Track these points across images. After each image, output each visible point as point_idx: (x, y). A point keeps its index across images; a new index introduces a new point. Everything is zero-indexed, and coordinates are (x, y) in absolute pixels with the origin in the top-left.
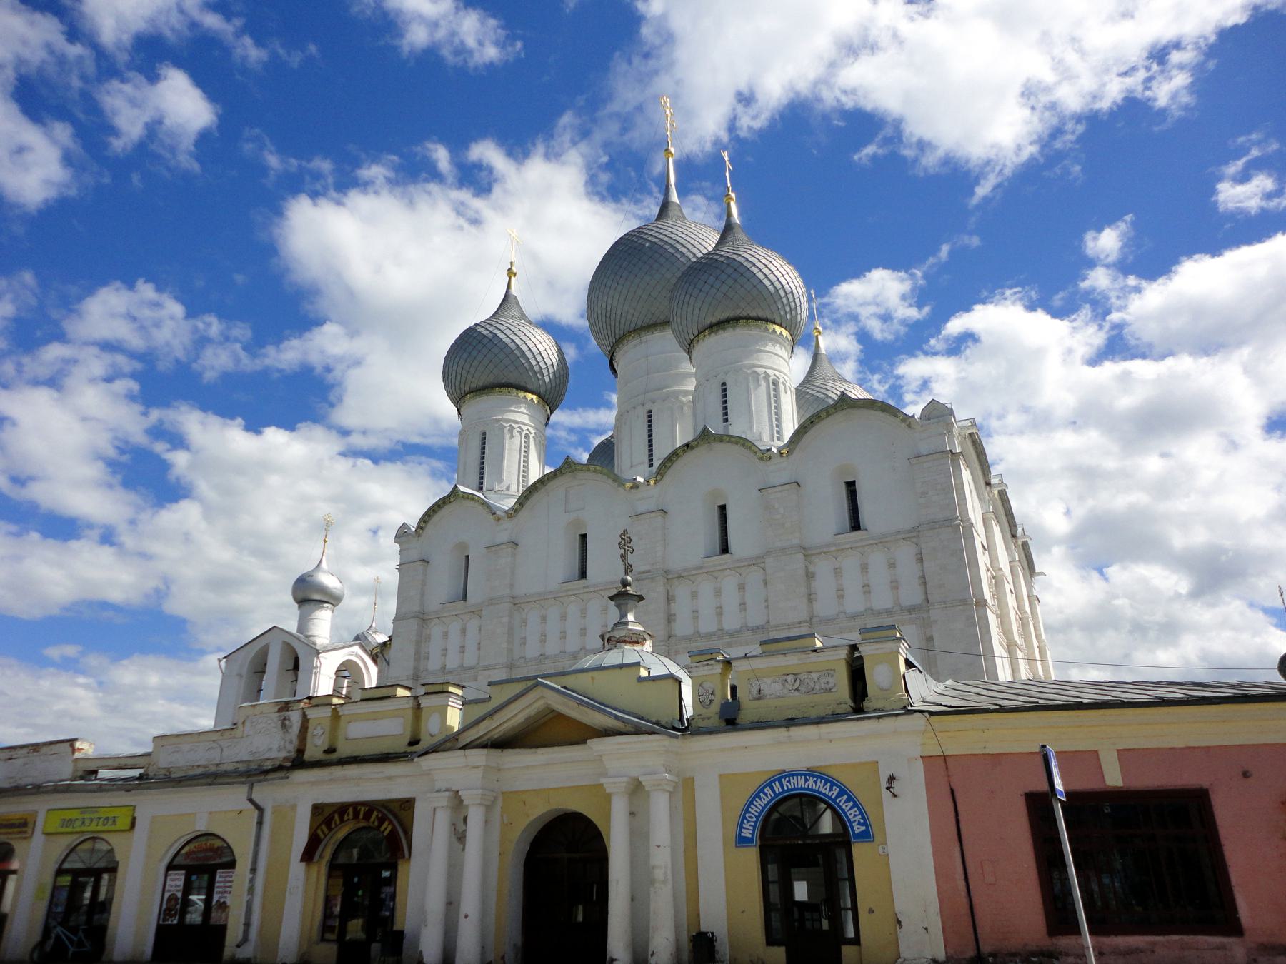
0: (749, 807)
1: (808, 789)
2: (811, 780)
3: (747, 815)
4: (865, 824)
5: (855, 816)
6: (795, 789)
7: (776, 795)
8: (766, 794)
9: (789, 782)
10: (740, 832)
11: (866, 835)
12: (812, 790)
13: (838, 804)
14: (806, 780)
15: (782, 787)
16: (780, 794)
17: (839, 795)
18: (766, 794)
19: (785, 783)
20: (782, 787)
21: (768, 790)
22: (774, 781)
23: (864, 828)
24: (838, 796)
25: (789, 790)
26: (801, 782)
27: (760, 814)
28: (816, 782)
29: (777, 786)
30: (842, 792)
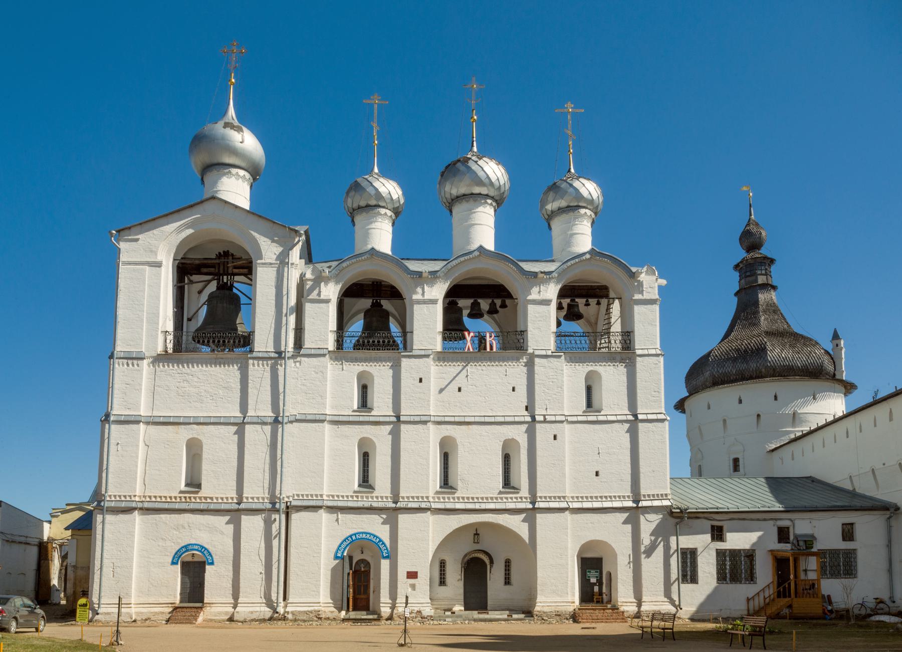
0: (341, 544)
2: (368, 535)
5: (385, 550)
8: (348, 540)
9: (359, 535)
10: (337, 554)
13: (378, 545)
14: (366, 535)
16: (355, 540)
17: (380, 541)
18: (348, 540)
23: (387, 555)
24: (378, 542)
28: (370, 536)
29: (354, 537)
30: (380, 540)
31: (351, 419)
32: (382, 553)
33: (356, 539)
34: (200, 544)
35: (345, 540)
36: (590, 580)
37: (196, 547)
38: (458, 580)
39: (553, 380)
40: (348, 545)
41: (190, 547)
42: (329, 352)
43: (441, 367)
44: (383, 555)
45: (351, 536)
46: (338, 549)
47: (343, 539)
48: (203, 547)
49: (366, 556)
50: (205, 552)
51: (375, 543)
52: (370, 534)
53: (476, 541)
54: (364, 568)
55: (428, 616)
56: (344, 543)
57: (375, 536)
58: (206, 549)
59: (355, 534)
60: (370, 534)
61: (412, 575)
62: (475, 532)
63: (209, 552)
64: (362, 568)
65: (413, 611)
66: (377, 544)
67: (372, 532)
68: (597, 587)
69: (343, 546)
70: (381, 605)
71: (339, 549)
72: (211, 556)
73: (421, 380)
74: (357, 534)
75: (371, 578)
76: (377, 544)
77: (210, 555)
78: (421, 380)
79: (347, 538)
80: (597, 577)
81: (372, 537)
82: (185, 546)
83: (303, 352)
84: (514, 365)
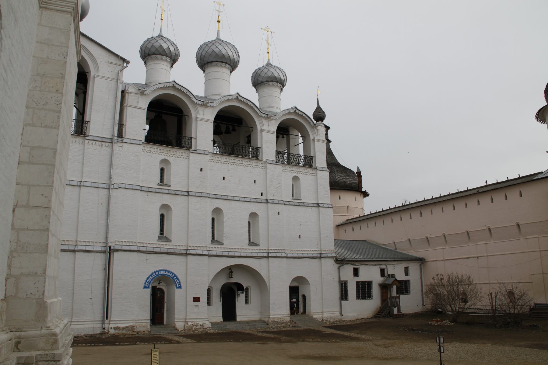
1: (166, 274)
2: (167, 272)
3: (148, 281)
5: (178, 282)
6: (162, 274)
7: (156, 276)
8: (153, 275)
11: (180, 287)
12: (167, 275)
14: (166, 272)
15: (159, 273)
16: (158, 275)
18: (153, 275)
19: (159, 272)
20: (159, 273)
22: (156, 272)
24: (174, 277)
25: (160, 274)
26: (164, 272)
27: (151, 281)
28: (168, 273)
29: (157, 273)
30: (175, 276)
31: (157, 190)
32: (176, 284)
33: (159, 275)
40: (153, 278)
42: (143, 143)
43: (213, 163)
44: (177, 286)
46: (146, 281)
49: (162, 286)
51: (172, 277)
52: (168, 271)
54: (159, 294)
55: (208, 327)
56: (151, 277)
57: (171, 273)
59: (158, 271)
60: (168, 271)
64: (158, 294)
65: (198, 325)
66: (173, 278)
67: (170, 270)
69: (149, 279)
70: (176, 320)
73: (201, 170)
74: (160, 271)
75: (165, 302)
76: (173, 278)
78: (201, 170)
81: (169, 273)
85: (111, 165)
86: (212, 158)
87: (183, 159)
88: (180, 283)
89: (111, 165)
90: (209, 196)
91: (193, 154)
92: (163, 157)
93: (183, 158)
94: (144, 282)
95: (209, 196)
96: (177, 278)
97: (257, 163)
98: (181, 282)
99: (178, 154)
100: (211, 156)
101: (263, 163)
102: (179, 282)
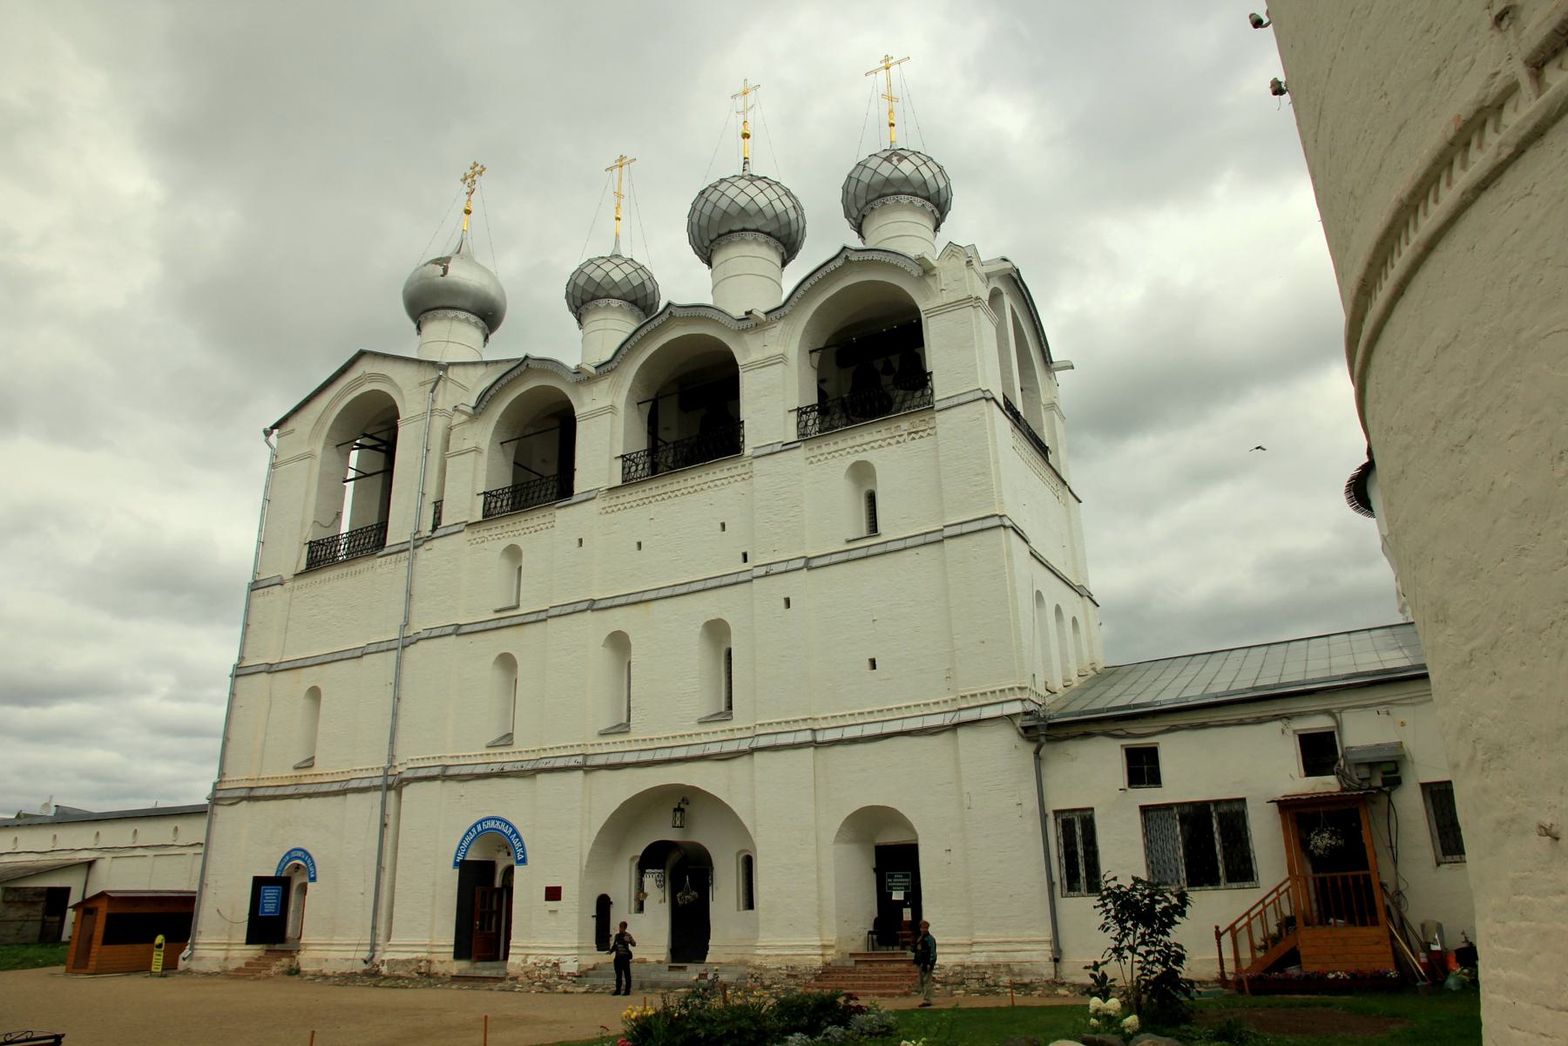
2: (498, 823)
4: (523, 854)
5: (520, 848)
16: (481, 832)
17: (512, 833)
19: (484, 825)
21: (474, 830)
26: (492, 824)
30: (514, 831)
33: (483, 831)
34: (306, 849)
35: (467, 834)
36: (891, 894)
37: (299, 854)
38: (660, 902)
39: (785, 496)
41: (293, 854)
45: (475, 826)
47: (465, 830)
48: (306, 853)
50: (309, 861)
53: (678, 823)
58: (310, 857)
59: (480, 822)
61: (553, 894)
62: (677, 807)
63: (312, 862)
68: (909, 910)
71: (459, 849)
72: (314, 868)
77: (313, 865)
79: (470, 830)
80: (906, 888)
82: (289, 853)
83: (438, 533)
84: (723, 484)
85: (409, 595)
86: (605, 504)
87: (547, 530)
88: (523, 850)
89: (409, 595)
90: (592, 606)
91: (563, 510)
92: (505, 543)
93: (547, 528)
94: (454, 852)
95: (592, 606)
96: (518, 836)
97: (728, 469)
98: (526, 845)
99: (536, 522)
100: (607, 499)
101: (747, 463)
102: (523, 847)
